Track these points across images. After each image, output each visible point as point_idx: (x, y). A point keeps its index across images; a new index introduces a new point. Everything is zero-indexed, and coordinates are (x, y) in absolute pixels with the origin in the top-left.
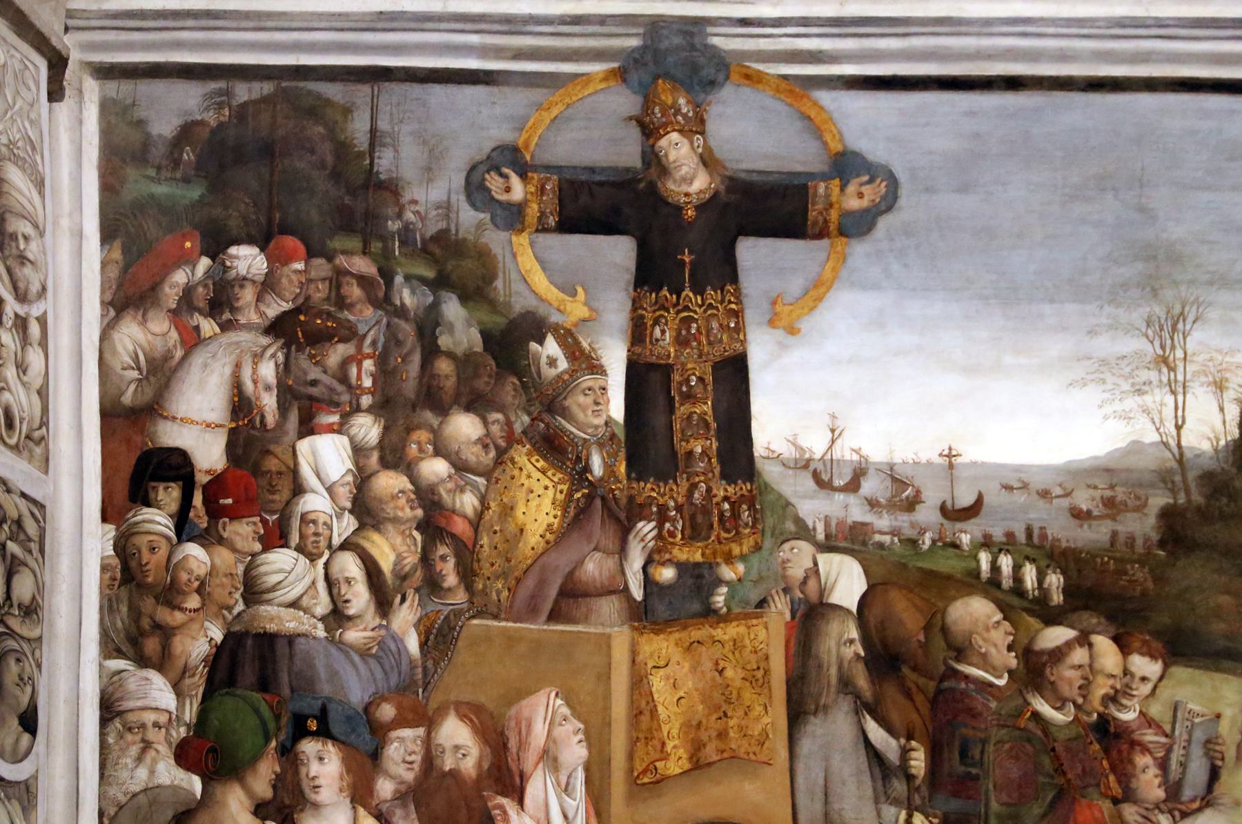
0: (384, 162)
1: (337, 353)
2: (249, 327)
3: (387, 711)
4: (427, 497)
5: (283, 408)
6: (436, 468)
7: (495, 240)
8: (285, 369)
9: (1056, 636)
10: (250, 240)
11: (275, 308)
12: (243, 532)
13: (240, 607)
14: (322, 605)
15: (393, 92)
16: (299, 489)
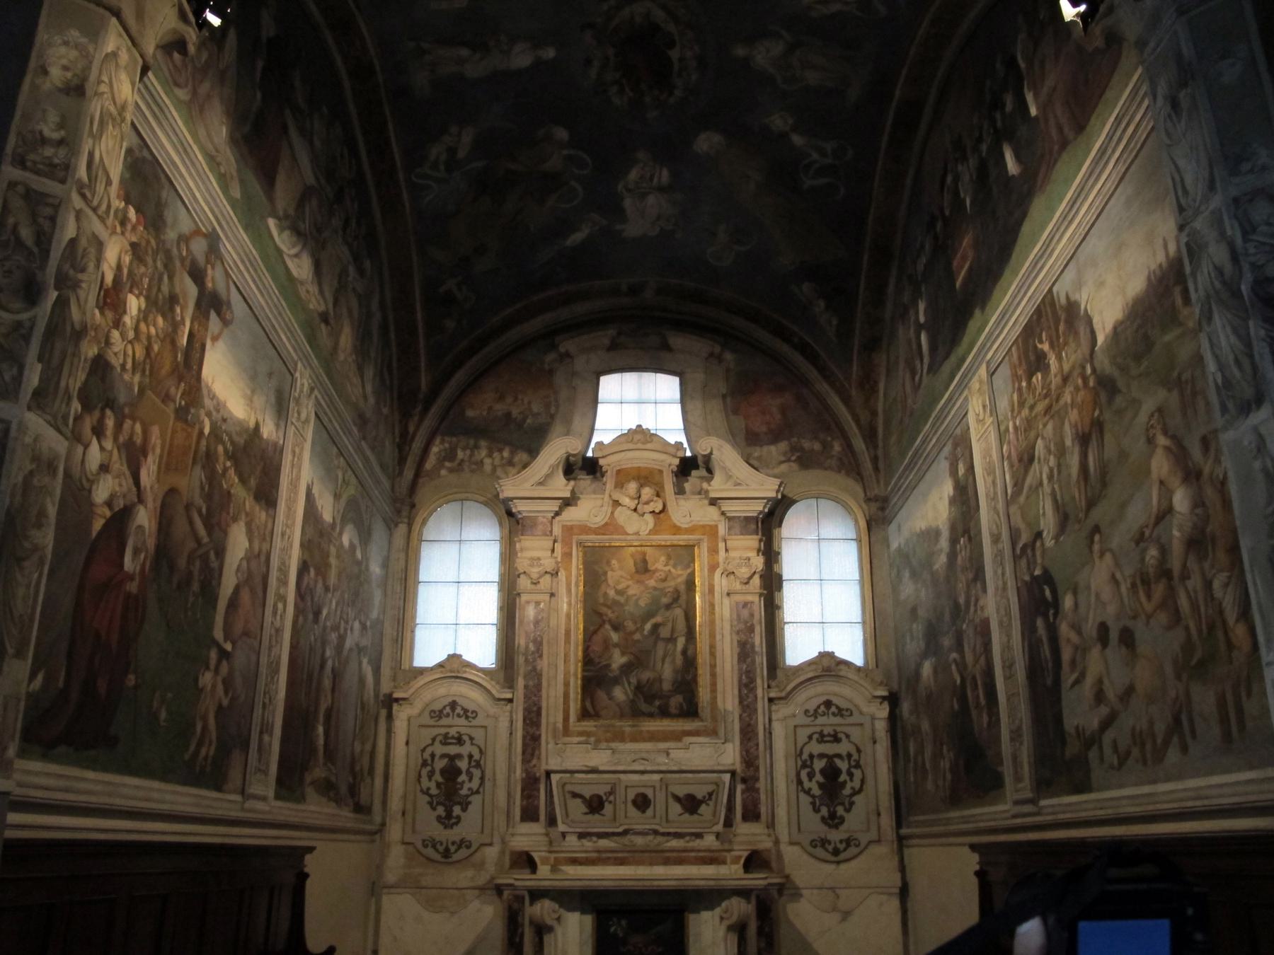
0: (166, 213)
1: (143, 269)
2: (126, 238)
3: (127, 410)
4: (149, 337)
5: (128, 279)
6: (153, 330)
7: (178, 264)
8: (131, 262)
9: (228, 464)
10: (135, 208)
11: (134, 239)
12: (110, 315)
13: (103, 345)
14: (121, 361)
15: (173, 193)
16: (125, 312)
